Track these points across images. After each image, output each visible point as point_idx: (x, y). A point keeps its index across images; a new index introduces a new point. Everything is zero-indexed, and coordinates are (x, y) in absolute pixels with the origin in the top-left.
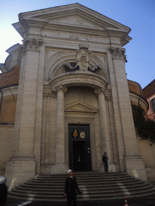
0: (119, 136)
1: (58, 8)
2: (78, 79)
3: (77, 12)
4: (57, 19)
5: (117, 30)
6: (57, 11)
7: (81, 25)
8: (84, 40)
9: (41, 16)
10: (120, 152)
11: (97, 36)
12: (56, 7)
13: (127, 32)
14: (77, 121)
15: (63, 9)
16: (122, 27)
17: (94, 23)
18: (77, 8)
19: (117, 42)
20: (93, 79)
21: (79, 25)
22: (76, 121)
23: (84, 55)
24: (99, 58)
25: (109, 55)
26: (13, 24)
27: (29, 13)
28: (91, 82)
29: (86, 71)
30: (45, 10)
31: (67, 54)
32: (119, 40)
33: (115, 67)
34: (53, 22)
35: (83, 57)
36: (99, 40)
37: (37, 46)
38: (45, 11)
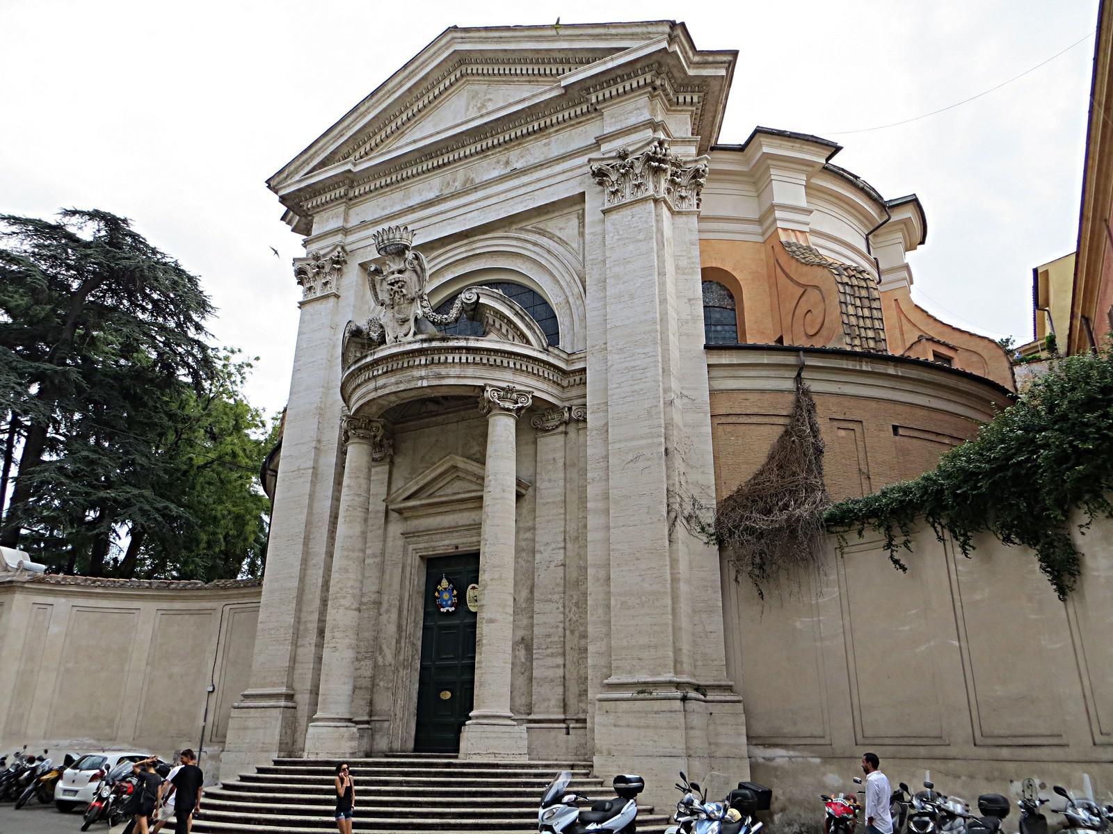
1: (380, 94)
2: (381, 382)
4: (396, 135)
5: (610, 65)
6: (384, 105)
7: (484, 111)
9: (334, 153)
10: (594, 666)
11: (547, 131)
12: (373, 94)
13: (664, 44)
14: (447, 542)
16: (633, 36)
17: (532, 78)
18: (451, 51)
19: (633, 120)
20: (432, 363)
22: (443, 545)
23: (396, 275)
24: (558, 233)
26: (283, 219)
27: (292, 168)
28: (422, 378)
29: (404, 340)
30: (340, 128)
32: (644, 100)
33: (608, 254)
35: (392, 284)
36: (557, 144)
37: (328, 278)
38: (339, 132)
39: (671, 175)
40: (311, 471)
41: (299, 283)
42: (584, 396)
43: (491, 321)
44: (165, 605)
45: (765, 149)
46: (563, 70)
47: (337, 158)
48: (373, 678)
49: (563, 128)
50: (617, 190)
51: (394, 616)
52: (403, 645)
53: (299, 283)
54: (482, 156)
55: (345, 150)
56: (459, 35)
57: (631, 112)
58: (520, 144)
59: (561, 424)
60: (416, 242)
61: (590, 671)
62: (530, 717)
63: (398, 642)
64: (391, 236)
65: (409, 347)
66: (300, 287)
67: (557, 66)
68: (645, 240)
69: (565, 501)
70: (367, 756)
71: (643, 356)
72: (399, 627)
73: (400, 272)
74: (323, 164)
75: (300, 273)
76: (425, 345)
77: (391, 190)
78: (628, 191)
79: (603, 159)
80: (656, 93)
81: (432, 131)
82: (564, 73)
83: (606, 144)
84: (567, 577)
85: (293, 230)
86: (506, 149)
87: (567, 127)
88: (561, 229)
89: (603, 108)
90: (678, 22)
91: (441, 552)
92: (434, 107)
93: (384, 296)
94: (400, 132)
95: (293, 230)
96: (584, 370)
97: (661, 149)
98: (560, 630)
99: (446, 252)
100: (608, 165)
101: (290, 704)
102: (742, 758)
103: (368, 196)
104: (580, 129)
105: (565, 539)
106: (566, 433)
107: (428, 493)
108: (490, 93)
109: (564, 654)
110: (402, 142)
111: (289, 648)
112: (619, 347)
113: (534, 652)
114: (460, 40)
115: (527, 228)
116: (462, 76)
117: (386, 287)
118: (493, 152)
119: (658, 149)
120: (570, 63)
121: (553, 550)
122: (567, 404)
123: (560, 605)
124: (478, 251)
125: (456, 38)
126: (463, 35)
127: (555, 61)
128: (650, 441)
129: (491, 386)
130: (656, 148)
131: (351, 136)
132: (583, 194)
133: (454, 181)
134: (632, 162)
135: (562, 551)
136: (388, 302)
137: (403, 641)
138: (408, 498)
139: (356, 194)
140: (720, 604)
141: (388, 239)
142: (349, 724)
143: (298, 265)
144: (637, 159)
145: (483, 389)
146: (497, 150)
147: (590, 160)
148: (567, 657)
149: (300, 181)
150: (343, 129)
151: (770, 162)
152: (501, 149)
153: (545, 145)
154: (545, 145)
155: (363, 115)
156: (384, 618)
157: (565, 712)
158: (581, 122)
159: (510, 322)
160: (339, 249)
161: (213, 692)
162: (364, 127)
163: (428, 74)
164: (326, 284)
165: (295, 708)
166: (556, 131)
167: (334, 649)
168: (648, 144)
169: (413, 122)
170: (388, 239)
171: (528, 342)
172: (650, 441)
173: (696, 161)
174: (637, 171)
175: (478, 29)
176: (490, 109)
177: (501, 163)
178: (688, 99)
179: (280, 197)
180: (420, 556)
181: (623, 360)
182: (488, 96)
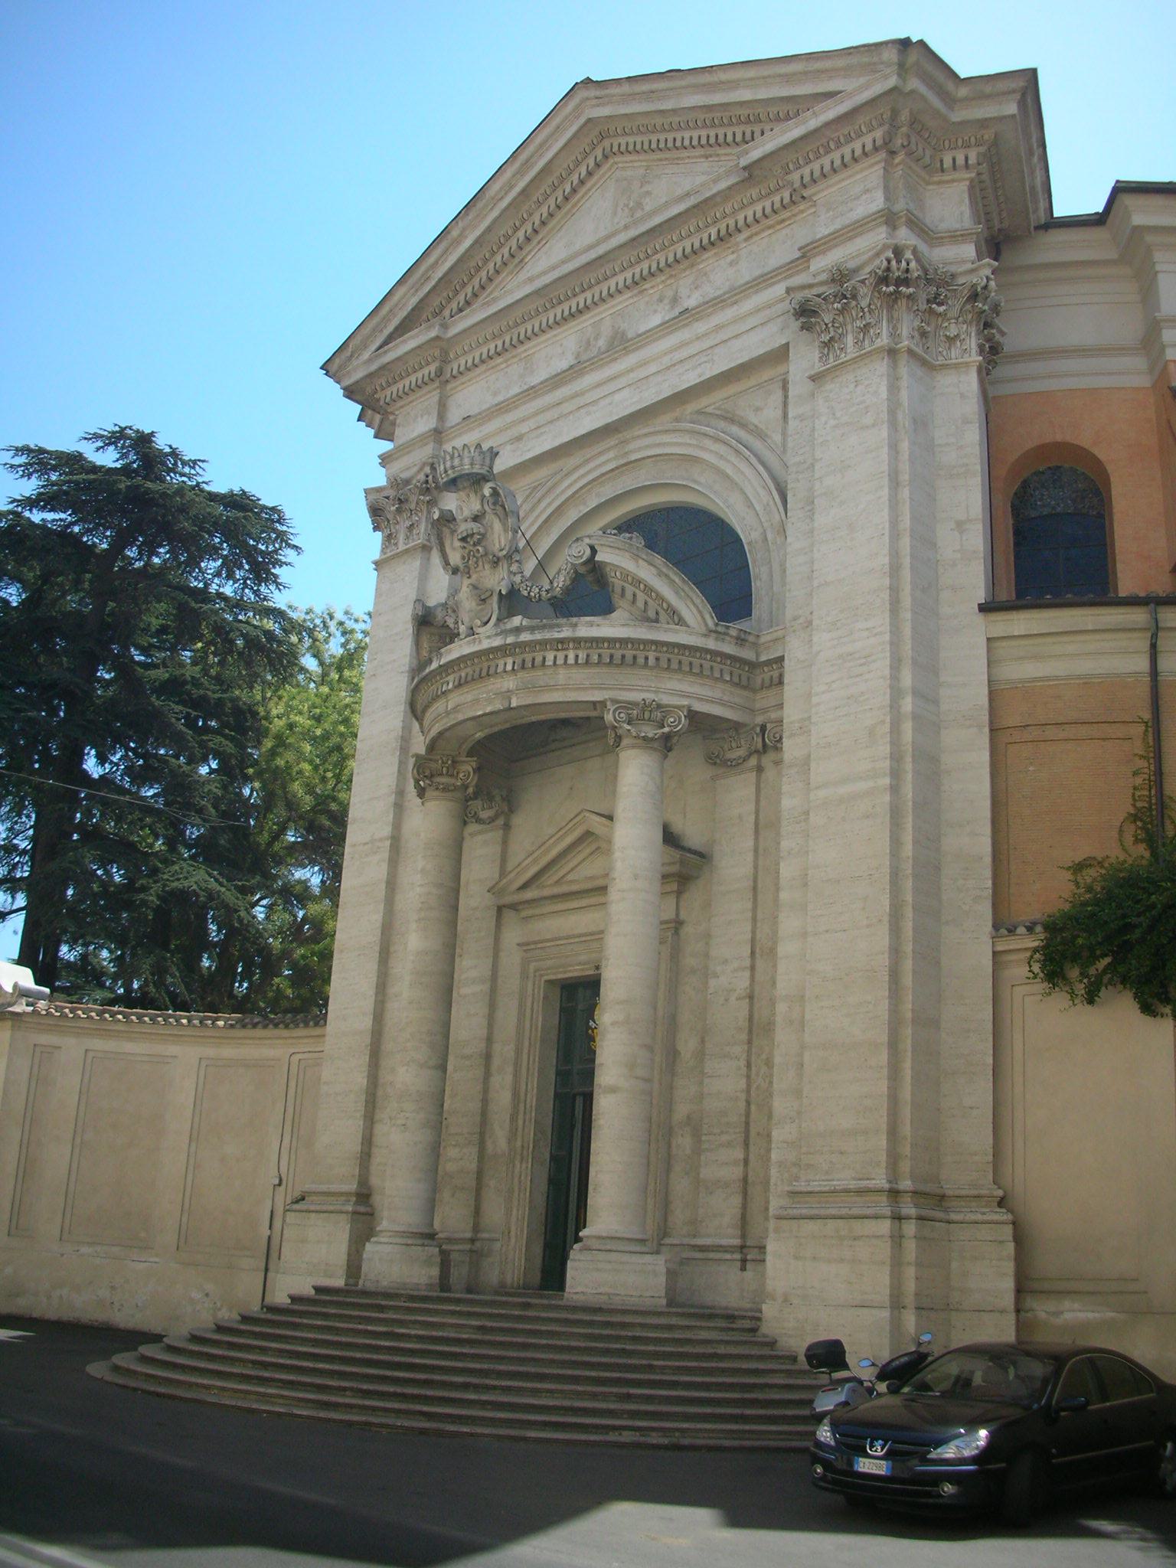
0: (784, 1038)
1: (480, 205)
3: (602, 137)
4: (511, 267)
5: (813, 123)
7: (639, 214)
8: (656, 320)
9: (417, 308)
13: (892, 81)
15: (510, 186)
16: (847, 72)
18: (582, 120)
21: (626, 227)
24: (753, 419)
25: (805, 359)
26: (358, 420)
31: (567, 487)
34: (488, 304)
35: (464, 539)
39: (928, 301)
40: (388, 843)
41: (375, 529)
42: (781, 706)
43: (618, 590)
44: (210, 1052)
45: (1137, 220)
46: (753, 133)
47: (424, 317)
48: (480, 1174)
49: (756, 234)
50: (832, 339)
51: (509, 1078)
52: (520, 1122)
53: (375, 529)
54: (635, 291)
55: (436, 302)
56: (593, 92)
57: (857, 198)
58: (692, 266)
59: (749, 756)
60: (500, 466)
61: (774, 1172)
62: (700, 1241)
63: (513, 1118)
64: (456, 462)
65: (486, 644)
66: (379, 534)
67: (742, 128)
68: (873, 426)
69: (755, 889)
70: (469, 1291)
71: (866, 634)
72: (515, 1094)
73: (476, 518)
74: (402, 329)
75: (376, 512)
76: (510, 640)
77: (506, 361)
78: (850, 340)
79: (810, 286)
80: (897, 161)
81: (563, 255)
82: (753, 139)
83: (818, 259)
84: (756, 1016)
85: (376, 437)
86: (671, 276)
87: (763, 230)
88: (758, 409)
89: (815, 194)
90: (914, 40)
91: (576, 974)
92: (567, 214)
93: (455, 558)
94: (516, 260)
95: (376, 437)
96: (781, 659)
97: (899, 262)
98: (742, 1104)
99: (587, 461)
100: (819, 296)
101: (362, 1209)
102: (1002, 1311)
103: (471, 374)
104: (784, 232)
105: (753, 953)
106: (760, 769)
107: (556, 878)
108: (648, 182)
109: (746, 1144)
110: (523, 276)
111: (361, 1123)
112: (829, 619)
113: (704, 1138)
114: (594, 102)
115: (707, 410)
116: (606, 157)
117: (458, 544)
118: (653, 283)
119: (894, 263)
120: (761, 122)
121: (735, 970)
122: (759, 720)
123: (742, 1063)
124: (633, 457)
125: (588, 99)
126: (598, 93)
127: (740, 122)
128: (871, 784)
129: (614, 701)
130: (889, 261)
131: (441, 279)
132: (787, 344)
133: (596, 339)
134: (854, 288)
135: (747, 974)
136: (462, 567)
137: (521, 1117)
138: (525, 886)
139: (455, 372)
140: (990, 1060)
141: (453, 467)
142: (426, 1242)
143: (372, 497)
144: (863, 282)
145: (603, 703)
146: (659, 280)
147: (788, 291)
148: (752, 1148)
149: (370, 360)
150: (427, 271)
151: (1149, 238)
152: (663, 278)
153: (731, 264)
154: (731, 264)
155: (457, 242)
156: (496, 1080)
157: (743, 1236)
158: (783, 221)
159: (649, 590)
160: (427, 470)
161: (280, 1185)
162: (460, 260)
163: (550, 162)
164: (411, 527)
165: (372, 1215)
166: (747, 239)
167: (403, 1128)
168: (878, 255)
169: (535, 242)
170: (453, 467)
171: (681, 622)
172: (871, 784)
173: (972, 271)
174: (864, 303)
175: (617, 81)
176: (648, 208)
177: (666, 301)
178: (960, 161)
179: (345, 389)
180: (546, 981)
181: (835, 642)
182: (645, 189)
